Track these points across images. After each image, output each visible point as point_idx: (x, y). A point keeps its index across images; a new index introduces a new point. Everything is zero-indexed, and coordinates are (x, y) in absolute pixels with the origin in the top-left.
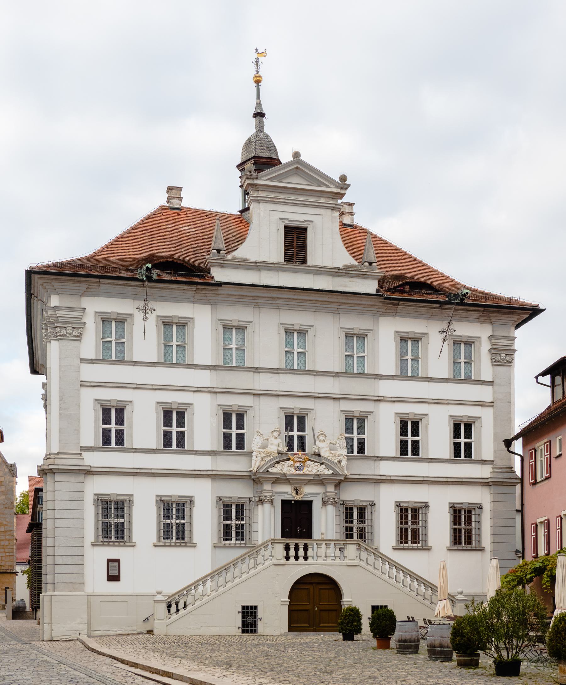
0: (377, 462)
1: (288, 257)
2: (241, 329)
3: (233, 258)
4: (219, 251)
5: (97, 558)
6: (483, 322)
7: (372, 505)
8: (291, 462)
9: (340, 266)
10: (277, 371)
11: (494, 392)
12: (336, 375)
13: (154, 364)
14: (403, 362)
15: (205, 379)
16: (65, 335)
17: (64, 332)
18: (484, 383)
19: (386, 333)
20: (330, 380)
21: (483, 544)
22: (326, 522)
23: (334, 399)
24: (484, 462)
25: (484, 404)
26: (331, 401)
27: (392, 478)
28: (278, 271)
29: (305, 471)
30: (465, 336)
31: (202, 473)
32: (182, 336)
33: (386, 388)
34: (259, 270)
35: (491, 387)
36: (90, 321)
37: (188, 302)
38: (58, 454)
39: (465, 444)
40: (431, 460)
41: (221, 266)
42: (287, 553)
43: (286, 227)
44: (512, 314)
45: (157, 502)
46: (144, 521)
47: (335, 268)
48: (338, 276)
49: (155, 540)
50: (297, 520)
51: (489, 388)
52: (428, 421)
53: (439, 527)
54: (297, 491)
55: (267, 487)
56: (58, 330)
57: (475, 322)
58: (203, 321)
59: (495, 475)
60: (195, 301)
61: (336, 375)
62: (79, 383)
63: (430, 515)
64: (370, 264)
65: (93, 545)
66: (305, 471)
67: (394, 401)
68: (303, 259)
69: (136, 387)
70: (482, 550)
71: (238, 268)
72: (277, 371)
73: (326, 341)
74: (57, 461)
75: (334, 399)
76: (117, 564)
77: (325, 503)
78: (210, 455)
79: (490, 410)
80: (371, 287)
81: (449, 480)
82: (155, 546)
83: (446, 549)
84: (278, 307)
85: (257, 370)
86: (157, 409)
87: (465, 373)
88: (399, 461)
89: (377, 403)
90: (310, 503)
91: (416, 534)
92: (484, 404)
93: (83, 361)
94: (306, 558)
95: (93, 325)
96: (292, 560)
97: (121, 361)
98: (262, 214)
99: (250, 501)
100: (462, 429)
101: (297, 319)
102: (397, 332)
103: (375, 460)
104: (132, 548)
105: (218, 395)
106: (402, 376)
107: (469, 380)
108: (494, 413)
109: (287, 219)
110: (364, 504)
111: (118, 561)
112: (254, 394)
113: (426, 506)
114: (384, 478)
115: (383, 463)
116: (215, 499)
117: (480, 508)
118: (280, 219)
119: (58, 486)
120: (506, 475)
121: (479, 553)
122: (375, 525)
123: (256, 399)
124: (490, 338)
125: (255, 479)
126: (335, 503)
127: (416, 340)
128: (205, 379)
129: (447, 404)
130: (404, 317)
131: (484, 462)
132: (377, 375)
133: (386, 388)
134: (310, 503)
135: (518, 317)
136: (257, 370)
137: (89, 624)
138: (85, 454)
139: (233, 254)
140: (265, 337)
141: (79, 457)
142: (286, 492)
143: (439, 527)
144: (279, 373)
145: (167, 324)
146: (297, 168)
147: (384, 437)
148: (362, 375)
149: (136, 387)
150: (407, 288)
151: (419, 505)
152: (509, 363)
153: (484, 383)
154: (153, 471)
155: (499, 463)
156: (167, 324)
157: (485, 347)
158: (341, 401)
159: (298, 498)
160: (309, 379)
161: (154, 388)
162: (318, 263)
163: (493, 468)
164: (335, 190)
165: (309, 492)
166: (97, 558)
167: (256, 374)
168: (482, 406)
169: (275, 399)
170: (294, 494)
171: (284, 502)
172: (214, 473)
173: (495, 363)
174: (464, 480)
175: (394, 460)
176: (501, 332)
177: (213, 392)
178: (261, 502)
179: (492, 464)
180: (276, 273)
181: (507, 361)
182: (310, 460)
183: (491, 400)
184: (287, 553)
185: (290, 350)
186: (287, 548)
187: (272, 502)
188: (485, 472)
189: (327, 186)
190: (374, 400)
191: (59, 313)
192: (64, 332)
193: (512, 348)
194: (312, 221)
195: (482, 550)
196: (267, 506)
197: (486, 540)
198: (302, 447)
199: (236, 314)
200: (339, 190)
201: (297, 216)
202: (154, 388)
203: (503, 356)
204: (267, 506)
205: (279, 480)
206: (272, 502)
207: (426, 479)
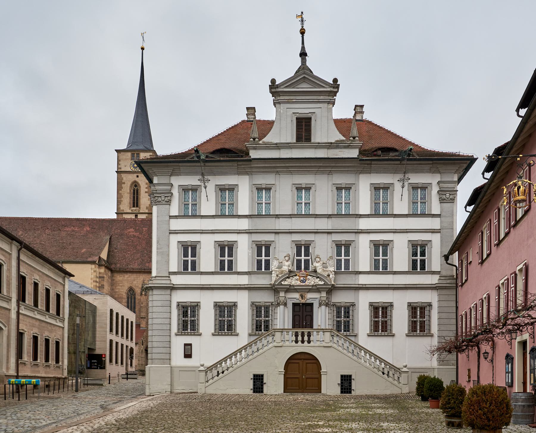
0: (357, 276)
1: (299, 138)
2: (268, 189)
3: (263, 142)
4: (254, 139)
5: (178, 343)
6: (433, 173)
7: (353, 305)
8: (298, 277)
9: (333, 141)
10: (290, 216)
11: (441, 222)
12: (329, 216)
13: (213, 217)
14: (376, 204)
15: (244, 224)
16: (160, 202)
17: (160, 199)
18: (434, 216)
19: (364, 186)
20: (325, 220)
21: (432, 332)
22: (322, 317)
23: (328, 233)
24: (434, 273)
25: (433, 231)
26: (325, 235)
27: (367, 286)
28: (291, 148)
29: (307, 283)
30: (420, 183)
31: (242, 286)
32: (231, 197)
33: (364, 224)
34: (279, 149)
35: (439, 218)
36: (175, 192)
37: (235, 174)
38: (156, 277)
39: (421, 260)
40: (395, 273)
41: (255, 148)
42: (297, 339)
43: (297, 119)
44: (454, 164)
45: (214, 306)
46: (207, 319)
47: (328, 143)
48: (332, 148)
50: (303, 316)
51: (438, 220)
52: (393, 245)
53: (400, 320)
54: (302, 296)
55: (282, 294)
56: (156, 198)
57: (428, 172)
58: (244, 185)
59: (441, 282)
60: (239, 174)
61: (329, 216)
62: (169, 232)
63: (394, 312)
64: (354, 138)
65: (176, 335)
66: (307, 283)
67: (369, 233)
68: (308, 139)
69: (202, 232)
70: (432, 336)
71: (266, 149)
72: (290, 216)
73: (323, 194)
74: (154, 282)
75: (328, 233)
76: (190, 347)
77: (320, 305)
78: (247, 274)
79: (438, 235)
80: (354, 153)
81: (407, 286)
82: (213, 335)
83: (405, 335)
84: (291, 173)
85: (277, 216)
86: (215, 246)
87: (421, 210)
88: (372, 274)
89: (357, 234)
90: (311, 305)
92: (433, 231)
93: (171, 217)
94: (309, 342)
95: (178, 194)
96: (300, 343)
97: (194, 216)
98: (282, 112)
99: (272, 304)
100: (419, 250)
101: (304, 180)
102: (371, 184)
103: (356, 274)
104: (199, 337)
105: (253, 234)
106: (376, 214)
107: (423, 215)
108: (441, 237)
109: (298, 113)
110: (348, 304)
111: (191, 345)
112: (276, 233)
113: (391, 305)
114: (361, 286)
115: (361, 276)
116: (250, 303)
117: (430, 305)
118: (293, 113)
119: (155, 298)
120: (449, 281)
121: (430, 338)
122: (355, 320)
123: (277, 236)
124: (439, 183)
125: (275, 289)
126: (327, 305)
127: (386, 188)
128: (244, 224)
129: (407, 232)
130: (377, 173)
131: (434, 273)
132: (357, 215)
133: (364, 224)
134: (311, 305)
135: (459, 166)
136: (277, 216)
137: (171, 385)
138: (172, 277)
139: (263, 140)
140: (283, 192)
141: (168, 278)
142: (295, 297)
143: (400, 320)
144: (291, 218)
145: (222, 189)
146: (304, 77)
147: (363, 258)
148: (348, 215)
149: (202, 232)
150: (380, 152)
151: (386, 305)
152: (453, 200)
153: (434, 216)
154: (211, 286)
155: (444, 273)
156: (222, 189)
157: (435, 190)
158: (333, 234)
159: (303, 301)
160: (312, 220)
161: (213, 232)
162: (318, 141)
163: (440, 276)
164: (329, 89)
165: (310, 297)
166: (178, 343)
167: (277, 219)
168: (432, 232)
169: (288, 236)
170: (300, 299)
171: (294, 305)
172: (249, 286)
173: (442, 201)
174: (418, 286)
175: (369, 274)
176: (447, 178)
177: (249, 232)
178: (278, 305)
179: (439, 274)
180: (290, 150)
181: (451, 199)
182: (311, 276)
183: (439, 228)
184: (297, 339)
185: (300, 201)
186: (297, 335)
187: (285, 305)
188: (434, 280)
189: (324, 87)
190: (356, 233)
191: (158, 188)
192: (160, 199)
193: (455, 189)
194: (314, 113)
195: (432, 336)
196: (282, 307)
198: (307, 267)
199: (263, 180)
200: (332, 89)
201: (304, 109)
202: (213, 232)
203: (448, 196)
204: (282, 307)
205: (290, 289)
206: (285, 305)
207: (390, 286)
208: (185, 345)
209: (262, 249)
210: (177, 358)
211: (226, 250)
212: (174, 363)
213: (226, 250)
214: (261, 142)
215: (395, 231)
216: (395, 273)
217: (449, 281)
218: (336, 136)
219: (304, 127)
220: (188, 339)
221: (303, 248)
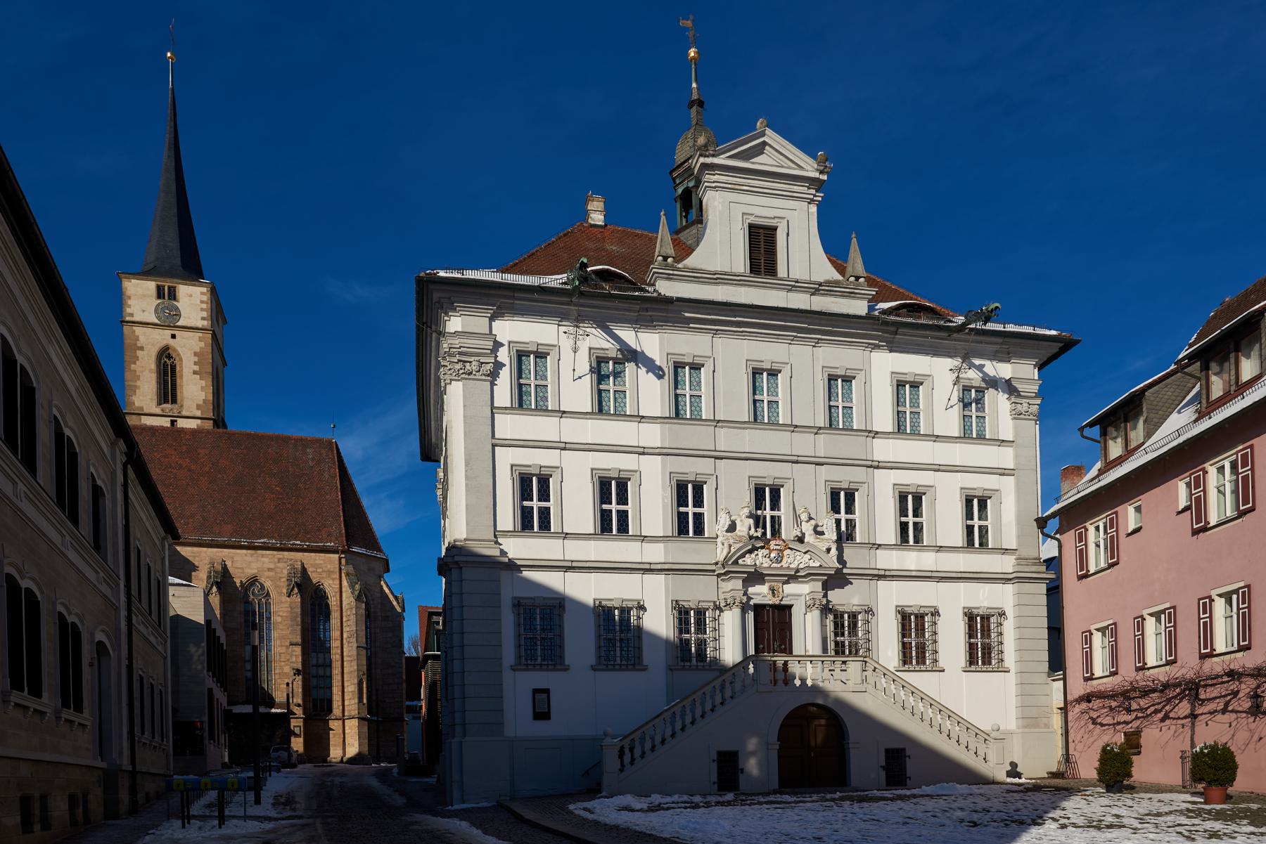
1: (755, 268)
4: (665, 258)
11: (1016, 456)
24: (1005, 551)
25: (1003, 472)
33: (884, 450)
40: (940, 549)
41: (669, 278)
49: (594, 663)
68: (771, 270)
76: (545, 696)
91: (921, 649)
92: (1003, 472)
101: (769, 350)
111: (547, 691)
120: (1034, 568)
128: (652, 435)
143: (951, 640)
147: (879, 516)
155: (1025, 553)
188: (1006, 564)
197: (1010, 658)
208: (536, 691)
209: (687, 493)
210: (518, 719)
211: (612, 490)
212: (509, 732)
213: (612, 490)
214: (680, 266)
215: (937, 468)
216: (940, 549)
217: (1034, 568)
218: (825, 271)
219: (762, 245)
220: (540, 679)
221: (765, 495)
